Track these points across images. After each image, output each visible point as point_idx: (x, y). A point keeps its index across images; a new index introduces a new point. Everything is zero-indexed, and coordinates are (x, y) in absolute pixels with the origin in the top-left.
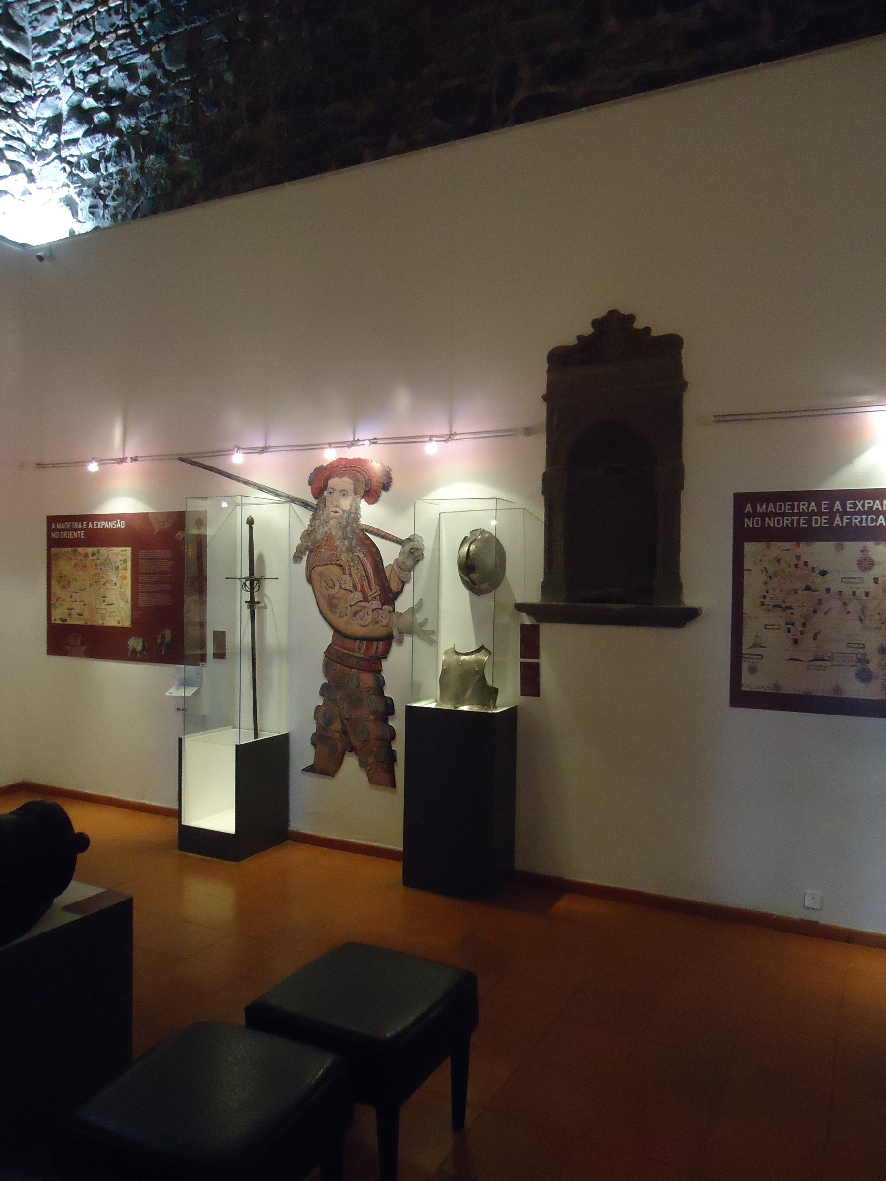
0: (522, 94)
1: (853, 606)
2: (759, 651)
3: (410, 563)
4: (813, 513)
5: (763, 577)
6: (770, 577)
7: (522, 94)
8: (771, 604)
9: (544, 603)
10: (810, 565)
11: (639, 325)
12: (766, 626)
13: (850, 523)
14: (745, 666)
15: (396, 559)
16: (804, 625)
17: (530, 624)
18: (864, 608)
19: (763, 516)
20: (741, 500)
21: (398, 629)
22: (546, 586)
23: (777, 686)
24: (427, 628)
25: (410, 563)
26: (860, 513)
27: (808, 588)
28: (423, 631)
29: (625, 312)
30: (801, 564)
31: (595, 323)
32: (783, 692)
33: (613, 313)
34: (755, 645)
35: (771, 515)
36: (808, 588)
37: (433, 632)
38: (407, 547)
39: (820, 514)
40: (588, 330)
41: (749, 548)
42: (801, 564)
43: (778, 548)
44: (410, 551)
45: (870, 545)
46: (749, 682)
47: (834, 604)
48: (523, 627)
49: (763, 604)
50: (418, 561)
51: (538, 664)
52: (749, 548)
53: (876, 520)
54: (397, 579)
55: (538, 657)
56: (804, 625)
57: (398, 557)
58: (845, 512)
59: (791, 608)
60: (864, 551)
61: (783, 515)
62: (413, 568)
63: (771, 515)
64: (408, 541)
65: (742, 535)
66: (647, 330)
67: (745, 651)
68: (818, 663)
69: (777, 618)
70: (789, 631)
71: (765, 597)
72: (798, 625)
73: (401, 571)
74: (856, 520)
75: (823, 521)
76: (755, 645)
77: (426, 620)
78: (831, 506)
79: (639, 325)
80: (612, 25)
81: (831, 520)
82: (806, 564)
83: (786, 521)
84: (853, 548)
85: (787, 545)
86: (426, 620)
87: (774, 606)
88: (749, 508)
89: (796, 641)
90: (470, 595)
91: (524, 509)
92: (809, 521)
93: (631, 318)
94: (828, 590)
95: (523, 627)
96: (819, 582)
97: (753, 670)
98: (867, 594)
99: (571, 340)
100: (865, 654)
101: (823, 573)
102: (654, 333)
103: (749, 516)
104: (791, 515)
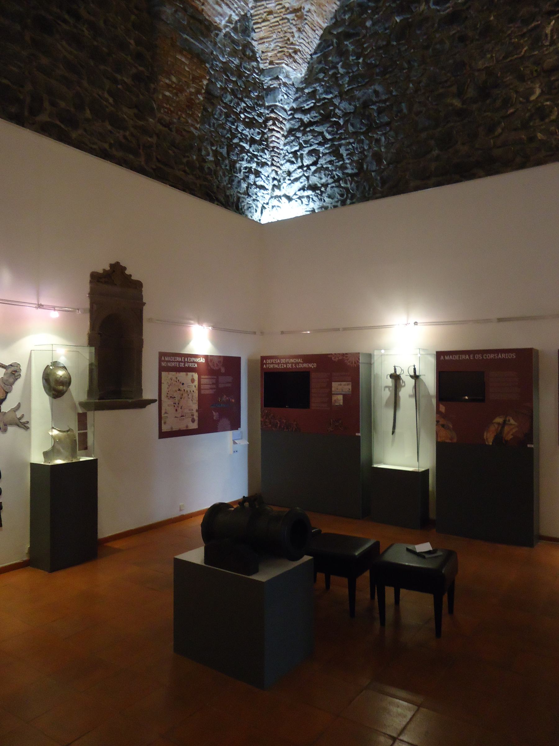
0: (44, 118)
1: (190, 396)
2: (166, 415)
3: (11, 380)
4: (179, 362)
5: (167, 386)
6: (169, 386)
7: (44, 118)
8: (169, 396)
9: (88, 401)
10: (180, 381)
11: (127, 272)
12: (168, 405)
13: (189, 366)
14: (163, 422)
15: (2, 378)
16: (178, 404)
17: (81, 412)
18: (193, 396)
19: (167, 361)
20: (162, 355)
21: (3, 422)
22: (90, 393)
23: (172, 428)
24: (23, 420)
25: (11, 380)
26: (191, 362)
27: (179, 390)
28: (21, 422)
29: (123, 264)
30: (177, 381)
31: (111, 266)
32: (173, 430)
33: (118, 263)
34: (166, 413)
35: (170, 361)
36: (179, 390)
37: (28, 422)
38: (10, 370)
39: (182, 362)
40: (108, 268)
41: (164, 374)
42: (177, 381)
43: (172, 374)
44: (12, 373)
45: (194, 373)
46: (165, 428)
47: (185, 395)
48: (79, 414)
49: (167, 396)
50: (17, 379)
51: (87, 432)
52: (164, 374)
53: (194, 365)
54: (3, 391)
55: (86, 429)
56: (178, 404)
57: (2, 376)
58: (188, 362)
59: (175, 397)
60: (192, 376)
61: (173, 362)
62: (13, 383)
63: (170, 361)
64: (10, 366)
65: (162, 369)
66: (131, 276)
67: (163, 416)
68: (182, 417)
69: (171, 402)
70: (174, 406)
71: (168, 394)
72: (177, 404)
73: (6, 386)
74: (190, 365)
75: (182, 365)
76: (166, 413)
77: (23, 416)
78: (184, 359)
79: (127, 272)
80: (88, 114)
81: (185, 364)
82: (179, 380)
83: (173, 364)
84: (190, 374)
85: (174, 373)
86: (23, 416)
87: (171, 397)
88: (163, 358)
89: (176, 410)
90: (49, 398)
91: (78, 352)
92: (179, 365)
93: (125, 268)
94: (184, 390)
95: (79, 414)
96: (182, 388)
97: (165, 423)
98: (193, 392)
99: (101, 271)
100: (193, 413)
101: (183, 384)
102: (133, 278)
103: (164, 361)
104: (175, 362)
